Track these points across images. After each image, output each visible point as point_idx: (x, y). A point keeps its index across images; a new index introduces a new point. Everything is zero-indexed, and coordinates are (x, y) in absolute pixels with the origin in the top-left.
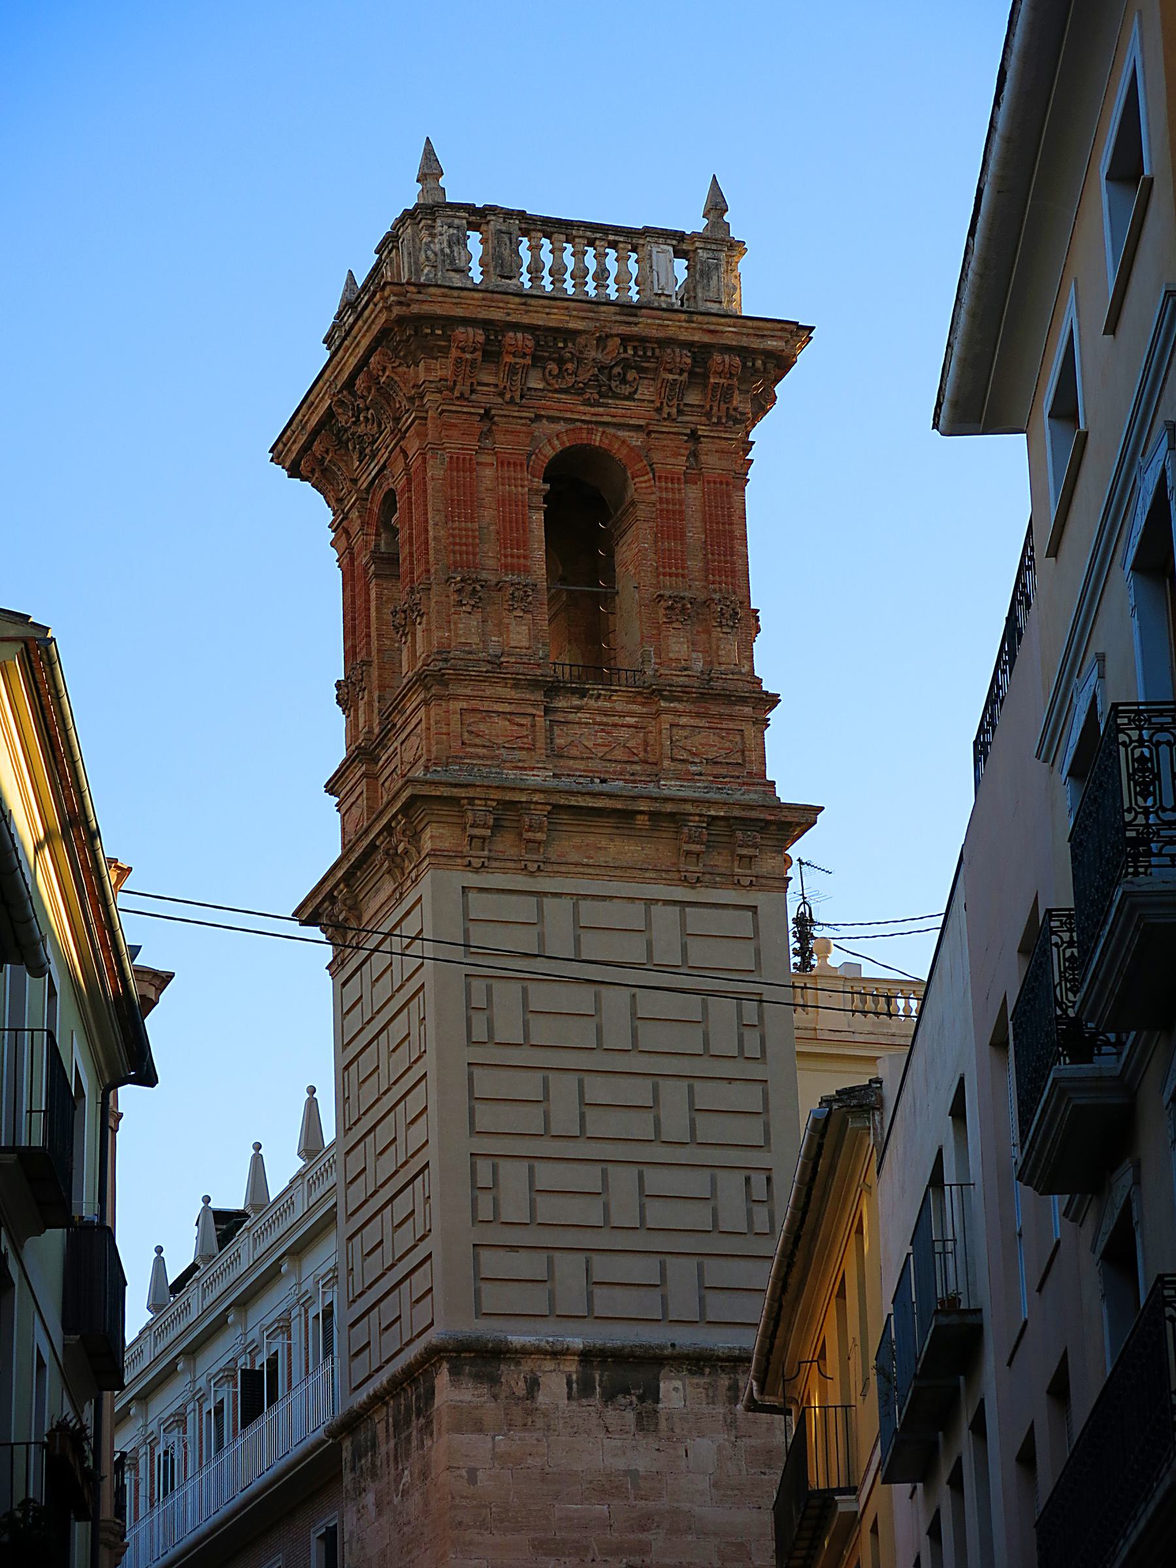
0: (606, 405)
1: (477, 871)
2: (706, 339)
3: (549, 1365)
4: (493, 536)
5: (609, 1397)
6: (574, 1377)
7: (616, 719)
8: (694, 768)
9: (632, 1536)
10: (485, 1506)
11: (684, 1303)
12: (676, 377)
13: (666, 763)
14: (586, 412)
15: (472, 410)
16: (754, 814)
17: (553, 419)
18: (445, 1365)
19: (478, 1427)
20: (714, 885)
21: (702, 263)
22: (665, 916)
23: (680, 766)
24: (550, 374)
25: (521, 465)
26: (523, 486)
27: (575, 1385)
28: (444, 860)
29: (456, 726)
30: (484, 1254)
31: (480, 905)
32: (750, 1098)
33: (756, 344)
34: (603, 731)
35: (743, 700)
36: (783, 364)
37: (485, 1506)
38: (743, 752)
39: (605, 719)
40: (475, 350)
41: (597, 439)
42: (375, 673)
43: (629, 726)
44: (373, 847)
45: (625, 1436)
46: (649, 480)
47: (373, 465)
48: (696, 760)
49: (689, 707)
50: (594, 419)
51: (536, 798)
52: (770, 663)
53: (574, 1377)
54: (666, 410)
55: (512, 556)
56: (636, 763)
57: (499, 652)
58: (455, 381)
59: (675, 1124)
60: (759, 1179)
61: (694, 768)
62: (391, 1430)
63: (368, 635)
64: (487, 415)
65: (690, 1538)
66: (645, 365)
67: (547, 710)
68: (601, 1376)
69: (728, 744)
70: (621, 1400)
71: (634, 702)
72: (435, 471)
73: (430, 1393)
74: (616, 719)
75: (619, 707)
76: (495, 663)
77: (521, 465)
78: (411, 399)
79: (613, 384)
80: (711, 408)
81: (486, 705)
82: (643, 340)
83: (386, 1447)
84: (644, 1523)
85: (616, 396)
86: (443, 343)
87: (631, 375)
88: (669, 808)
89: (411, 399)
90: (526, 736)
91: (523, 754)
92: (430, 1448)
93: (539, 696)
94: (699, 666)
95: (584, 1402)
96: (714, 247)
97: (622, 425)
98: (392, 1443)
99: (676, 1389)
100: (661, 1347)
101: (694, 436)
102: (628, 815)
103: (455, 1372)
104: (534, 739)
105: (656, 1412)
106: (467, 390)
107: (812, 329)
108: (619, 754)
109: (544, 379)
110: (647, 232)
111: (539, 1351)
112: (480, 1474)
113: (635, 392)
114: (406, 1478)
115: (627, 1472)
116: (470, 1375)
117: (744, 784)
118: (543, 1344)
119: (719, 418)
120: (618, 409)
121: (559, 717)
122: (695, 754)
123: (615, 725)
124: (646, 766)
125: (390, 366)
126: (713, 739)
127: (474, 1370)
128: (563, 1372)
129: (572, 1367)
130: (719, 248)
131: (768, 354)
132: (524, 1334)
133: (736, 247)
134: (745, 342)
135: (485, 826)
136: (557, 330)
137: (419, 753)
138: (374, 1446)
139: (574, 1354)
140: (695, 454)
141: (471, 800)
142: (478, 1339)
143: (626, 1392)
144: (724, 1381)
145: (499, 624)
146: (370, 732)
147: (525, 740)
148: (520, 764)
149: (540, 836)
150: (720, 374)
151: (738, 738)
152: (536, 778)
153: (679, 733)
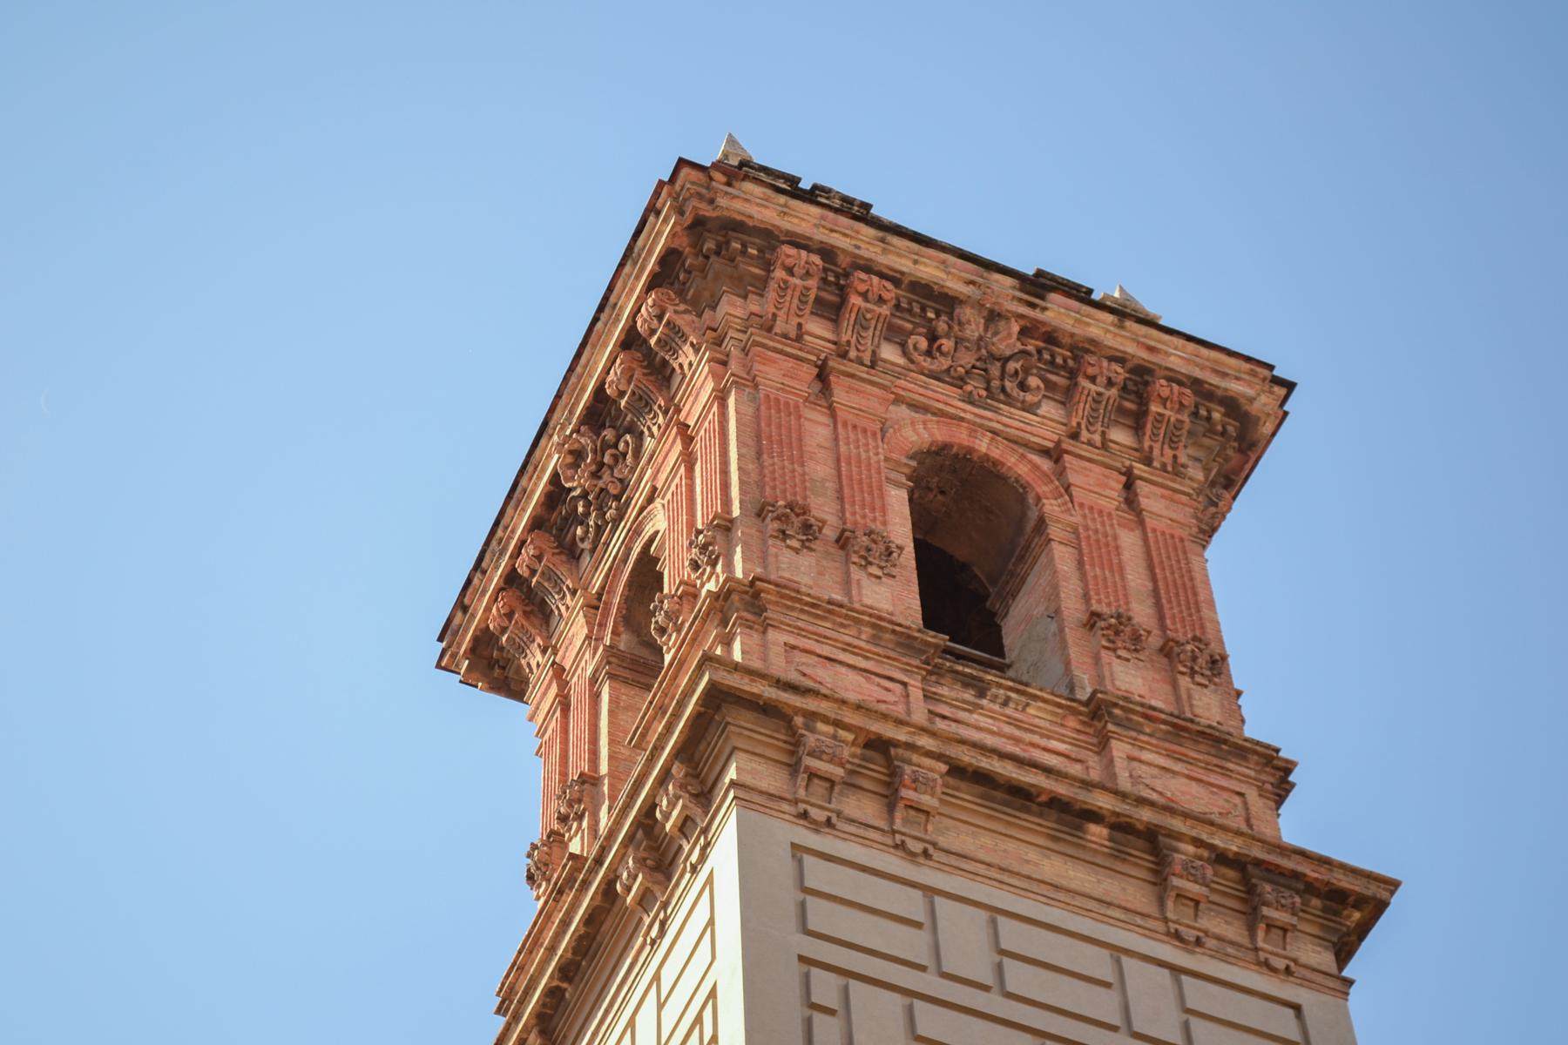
0: (996, 410)
1: (816, 827)
2: (1144, 355)
7: (1036, 739)
12: (1101, 390)
14: (969, 412)
17: (914, 406)
20: (1225, 958)
22: (1148, 986)
24: (915, 348)
28: (757, 798)
33: (1215, 380)
40: (808, 274)
41: (983, 445)
46: (1065, 503)
51: (924, 741)
54: (1085, 435)
58: (774, 315)
67: (928, 697)
74: (1036, 739)
79: (1008, 384)
80: (1151, 448)
81: (826, 650)
85: (1010, 400)
86: (757, 271)
87: (1033, 381)
88: (1146, 815)
109: (905, 353)
119: (1164, 466)
120: (1012, 419)
125: (671, 308)
131: (1232, 405)
134: (1198, 373)
141: (812, 716)
149: (926, 800)
150: (1164, 401)
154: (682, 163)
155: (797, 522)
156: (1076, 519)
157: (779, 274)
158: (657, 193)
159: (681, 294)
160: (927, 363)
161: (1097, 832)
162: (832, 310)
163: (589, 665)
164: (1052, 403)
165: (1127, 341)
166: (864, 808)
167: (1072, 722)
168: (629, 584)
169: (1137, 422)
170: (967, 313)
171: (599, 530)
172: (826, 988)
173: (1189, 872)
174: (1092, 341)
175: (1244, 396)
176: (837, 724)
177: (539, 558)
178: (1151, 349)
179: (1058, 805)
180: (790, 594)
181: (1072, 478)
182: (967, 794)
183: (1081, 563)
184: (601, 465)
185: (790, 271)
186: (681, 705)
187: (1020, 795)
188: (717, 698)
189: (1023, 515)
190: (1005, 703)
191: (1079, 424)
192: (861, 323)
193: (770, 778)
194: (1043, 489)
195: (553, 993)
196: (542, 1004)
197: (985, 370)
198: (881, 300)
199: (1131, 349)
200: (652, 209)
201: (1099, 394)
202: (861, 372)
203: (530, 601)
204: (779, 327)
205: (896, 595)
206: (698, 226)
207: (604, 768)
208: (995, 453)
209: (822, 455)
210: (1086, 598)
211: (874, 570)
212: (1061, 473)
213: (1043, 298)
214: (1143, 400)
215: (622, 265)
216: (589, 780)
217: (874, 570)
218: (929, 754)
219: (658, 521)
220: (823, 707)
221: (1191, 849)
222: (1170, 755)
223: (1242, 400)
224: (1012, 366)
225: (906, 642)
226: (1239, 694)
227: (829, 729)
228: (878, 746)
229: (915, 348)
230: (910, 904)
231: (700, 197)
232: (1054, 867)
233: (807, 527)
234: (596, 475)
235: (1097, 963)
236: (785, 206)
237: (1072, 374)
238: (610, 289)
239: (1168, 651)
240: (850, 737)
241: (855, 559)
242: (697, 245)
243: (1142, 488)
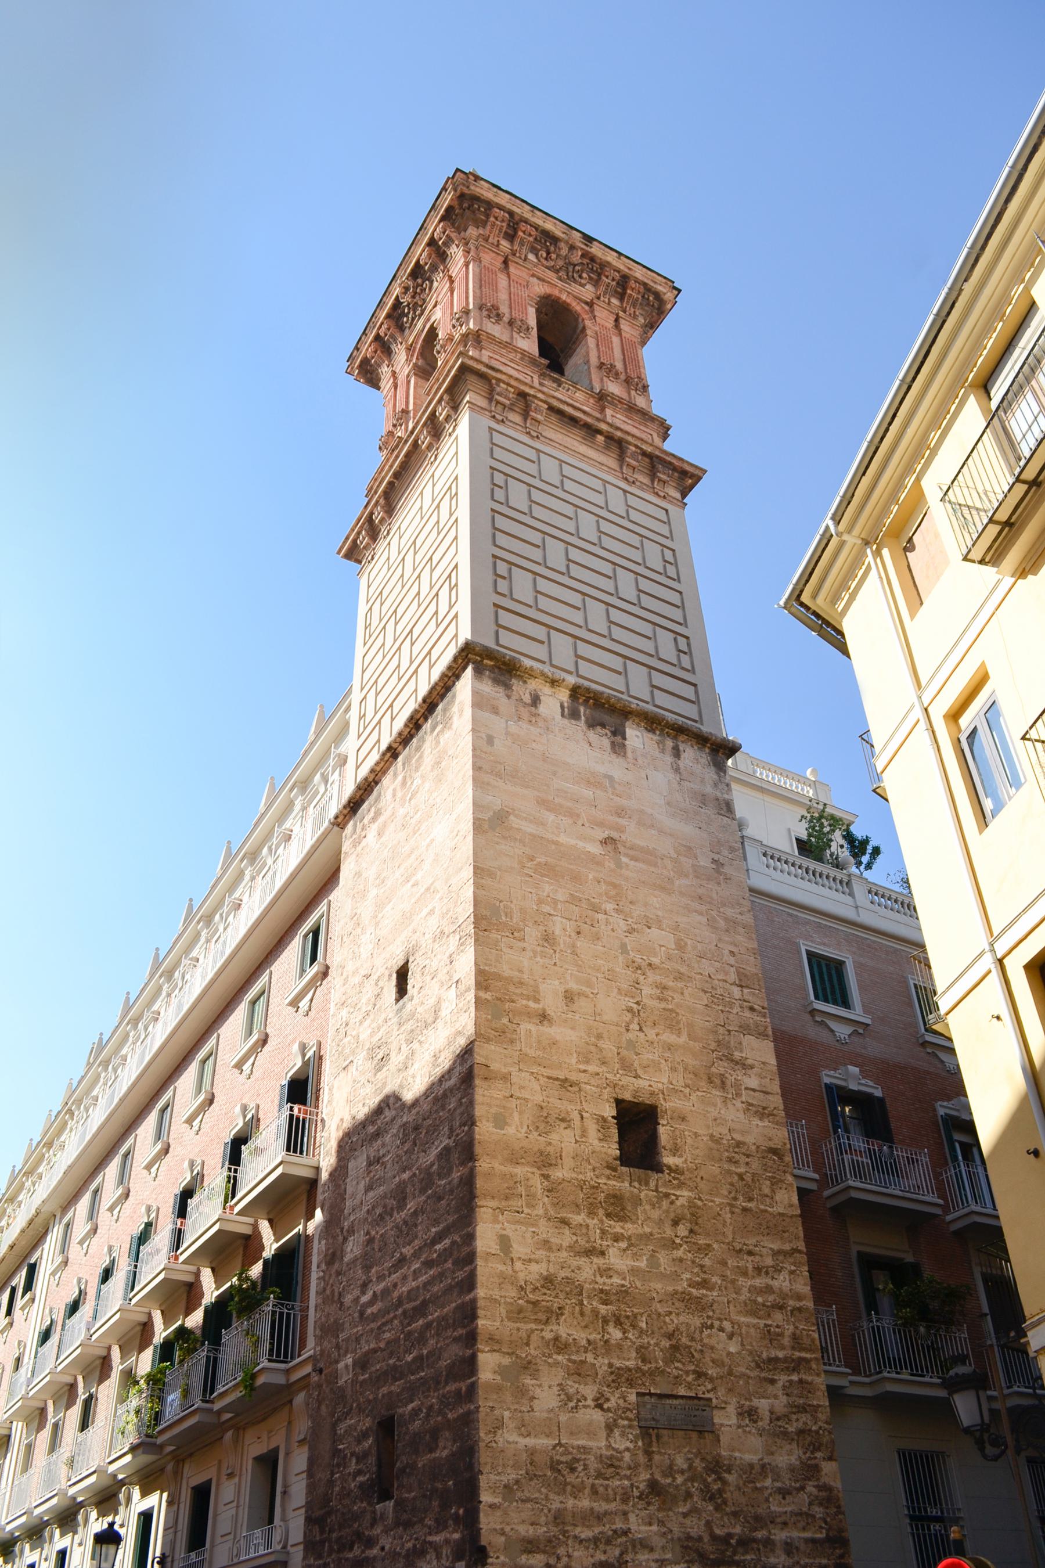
1: (498, 422)
2: (627, 270)
3: (546, 690)
5: (591, 725)
6: (566, 705)
10: (500, 763)
14: (560, 284)
16: (668, 458)
17: (539, 279)
18: (469, 670)
19: (495, 711)
20: (643, 490)
33: (652, 284)
37: (500, 763)
40: (503, 221)
41: (564, 297)
51: (540, 395)
81: (503, 360)
84: (620, 812)
85: (575, 281)
87: (585, 275)
88: (619, 434)
95: (573, 722)
99: (637, 736)
103: (478, 672)
105: (624, 745)
109: (537, 257)
112: (496, 741)
115: (606, 776)
116: (489, 677)
120: (575, 288)
129: (564, 695)
131: (657, 295)
141: (499, 380)
143: (603, 726)
144: (669, 743)
149: (539, 417)
150: (633, 289)
154: (458, 170)
155: (494, 312)
156: (597, 328)
157: (492, 219)
158: (447, 182)
159: (453, 225)
160: (545, 262)
161: (600, 438)
162: (511, 237)
163: (407, 370)
165: (620, 264)
166: (517, 418)
167: (592, 401)
168: (424, 340)
169: (621, 297)
170: (562, 245)
171: (413, 319)
172: (499, 479)
173: (633, 456)
174: (608, 263)
176: (508, 384)
177: (389, 329)
178: (630, 269)
179: (587, 426)
180: (491, 338)
181: (596, 313)
182: (554, 418)
183: (598, 345)
184: (415, 293)
185: (496, 218)
186: (449, 371)
187: (573, 421)
188: (464, 369)
189: (576, 327)
190: (568, 390)
192: (522, 243)
193: (482, 402)
194: (585, 316)
195: (391, 484)
196: (386, 488)
198: (530, 235)
199: (622, 267)
200: (444, 189)
202: (521, 262)
203: (384, 347)
204: (491, 240)
205: (530, 345)
206: (462, 197)
207: (411, 407)
208: (568, 301)
210: (599, 357)
212: (592, 311)
214: (624, 289)
215: (430, 212)
216: (405, 412)
218: (541, 400)
219: (437, 314)
220: (503, 377)
221: (634, 449)
222: (627, 417)
224: (577, 268)
225: (533, 362)
227: (505, 386)
228: (522, 395)
230: (532, 454)
231: (464, 185)
232: (583, 449)
233: (498, 315)
234: (413, 297)
235: (598, 485)
237: (599, 275)
238: (425, 221)
239: (628, 381)
240: (512, 390)
242: (461, 205)
243: (622, 321)
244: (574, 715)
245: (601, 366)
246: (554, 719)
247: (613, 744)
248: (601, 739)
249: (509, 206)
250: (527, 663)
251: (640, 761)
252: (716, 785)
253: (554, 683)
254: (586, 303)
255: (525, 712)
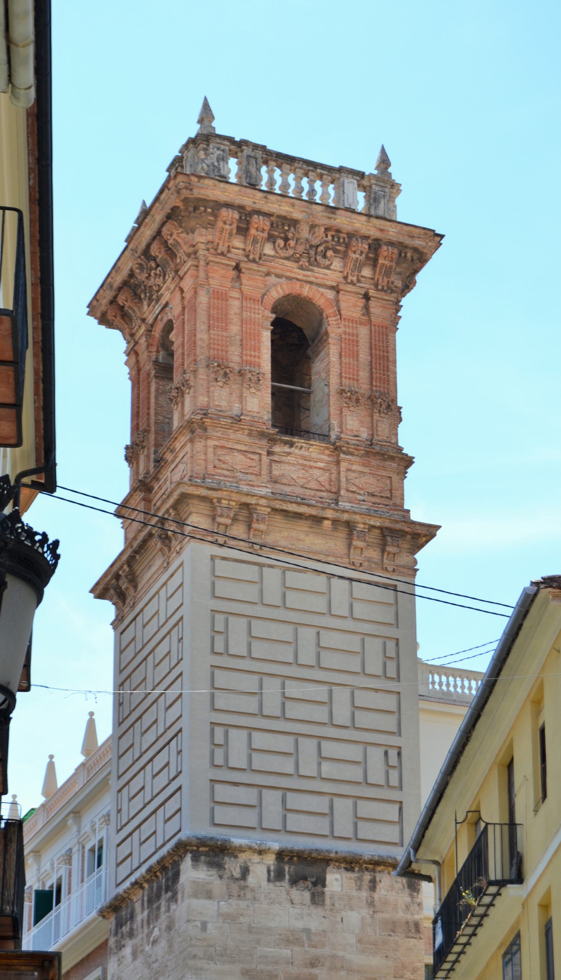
0: (312, 271)
2: (378, 235)
3: (256, 858)
4: (238, 342)
5: (294, 882)
6: (272, 868)
7: (312, 463)
8: (360, 497)
9: (306, 970)
11: (343, 826)
13: (343, 492)
15: (228, 262)
17: (278, 276)
21: (375, 193)
23: (351, 495)
24: (279, 246)
25: (258, 301)
26: (259, 314)
27: (272, 873)
29: (210, 456)
30: (218, 787)
31: (222, 568)
32: (389, 703)
33: (408, 241)
34: (303, 469)
35: (392, 458)
36: (421, 259)
38: (391, 490)
39: (305, 462)
41: (306, 291)
42: (152, 437)
43: (320, 468)
44: (150, 535)
45: (303, 907)
47: (157, 306)
48: (362, 492)
49: (358, 459)
50: (304, 278)
52: (407, 439)
53: (272, 868)
54: (350, 278)
55: (250, 356)
56: (323, 491)
57: (239, 413)
59: (342, 715)
60: (393, 753)
61: (360, 497)
62: (146, 904)
63: (148, 414)
64: (237, 268)
65: (343, 973)
66: (339, 248)
67: (269, 453)
68: (289, 868)
69: (381, 485)
70: (301, 884)
71: (323, 454)
72: (203, 298)
73: (177, 875)
74: (312, 463)
75: (314, 455)
76: (237, 420)
77: (258, 301)
78: (189, 255)
81: (229, 445)
82: (338, 231)
83: (141, 916)
85: (318, 265)
87: (330, 253)
88: (346, 517)
89: (189, 255)
90: (255, 467)
91: (252, 478)
92: (174, 911)
93: (264, 442)
94: (364, 434)
95: (278, 884)
96: (382, 184)
97: (322, 284)
98: (146, 913)
99: (337, 880)
100: (328, 851)
101: (367, 297)
102: (318, 520)
104: (260, 469)
105: (323, 893)
106: (225, 249)
107: (442, 236)
108: (313, 485)
110: (341, 170)
111: (250, 848)
113: (331, 264)
114: (156, 932)
117: (391, 509)
118: (253, 845)
120: (319, 274)
121: (276, 458)
122: (361, 489)
123: (311, 467)
124: (330, 494)
126: (372, 480)
127: (208, 859)
128: (264, 864)
129: (270, 860)
130: (386, 185)
131: (415, 250)
132: (242, 838)
133: (395, 187)
134: (402, 239)
135: (228, 517)
136: (285, 218)
137: (185, 473)
138: (132, 917)
139: (272, 853)
140: (366, 308)
141: (219, 500)
142: (211, 839)
143: (305, 879)
145: (241, 396)
146: (147, 473)
147: (254, 469)
148: (251, 483)
151: (388, 482)
152: (263, 491)
153: (352, 475)
155: (222, 372)
157: (220, 224)
160: (283, 253)
164: (338, 259)
166: (239, 530)
167: (327, 452)
169: (374, 262)
175: (421, 245)
178: (381, 230)
181: (343, 305)
182: (278, 517)
185: (225, 223)
187: (299, 516)
190: (301, 448)
191: (348, 273)
194: (329, 311)
197: (308, 254)
201: (357, 258)
208: (311, 295)
209: (236, 320)
211: (253, 390)
212: (338, 301)
213: (334, 213)
217: (253, 390)
223: (420, 248)
224: (321, 248)
225: (262, 435)
226: (400, 408)
229: (279, 246)
236: (224, 188)
237: (347, 246)
240: (234, 504)
241: (245, 386)
243: (373, 304)
244: (279, 875)
245: (342, 392)
246: (260, 887)
247: (313, 895)
248: (301, 895)
249: (238, 201)
250: (238, 839)
251: (337, 905)
252: (407, 907)
253: (260, 852)
254: (332, 288)
255: (235, 888)
